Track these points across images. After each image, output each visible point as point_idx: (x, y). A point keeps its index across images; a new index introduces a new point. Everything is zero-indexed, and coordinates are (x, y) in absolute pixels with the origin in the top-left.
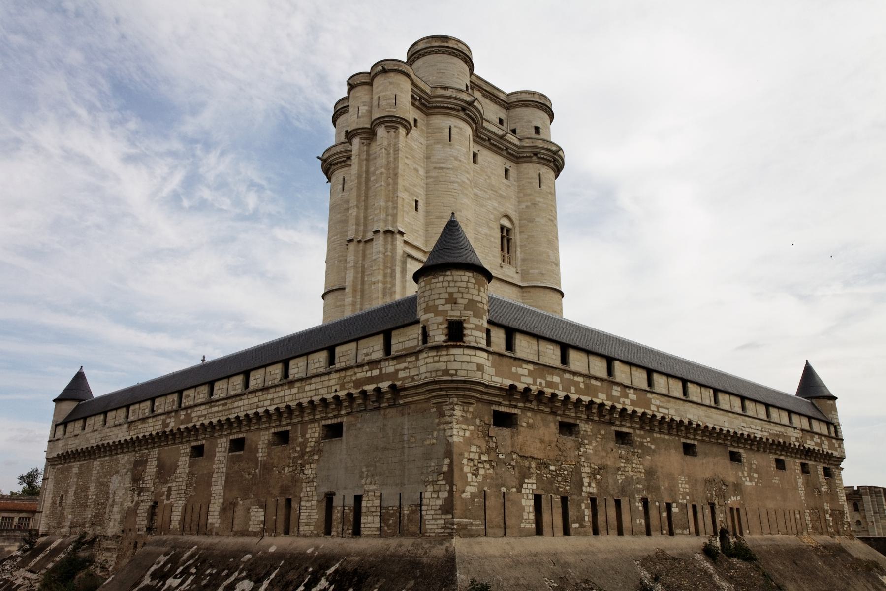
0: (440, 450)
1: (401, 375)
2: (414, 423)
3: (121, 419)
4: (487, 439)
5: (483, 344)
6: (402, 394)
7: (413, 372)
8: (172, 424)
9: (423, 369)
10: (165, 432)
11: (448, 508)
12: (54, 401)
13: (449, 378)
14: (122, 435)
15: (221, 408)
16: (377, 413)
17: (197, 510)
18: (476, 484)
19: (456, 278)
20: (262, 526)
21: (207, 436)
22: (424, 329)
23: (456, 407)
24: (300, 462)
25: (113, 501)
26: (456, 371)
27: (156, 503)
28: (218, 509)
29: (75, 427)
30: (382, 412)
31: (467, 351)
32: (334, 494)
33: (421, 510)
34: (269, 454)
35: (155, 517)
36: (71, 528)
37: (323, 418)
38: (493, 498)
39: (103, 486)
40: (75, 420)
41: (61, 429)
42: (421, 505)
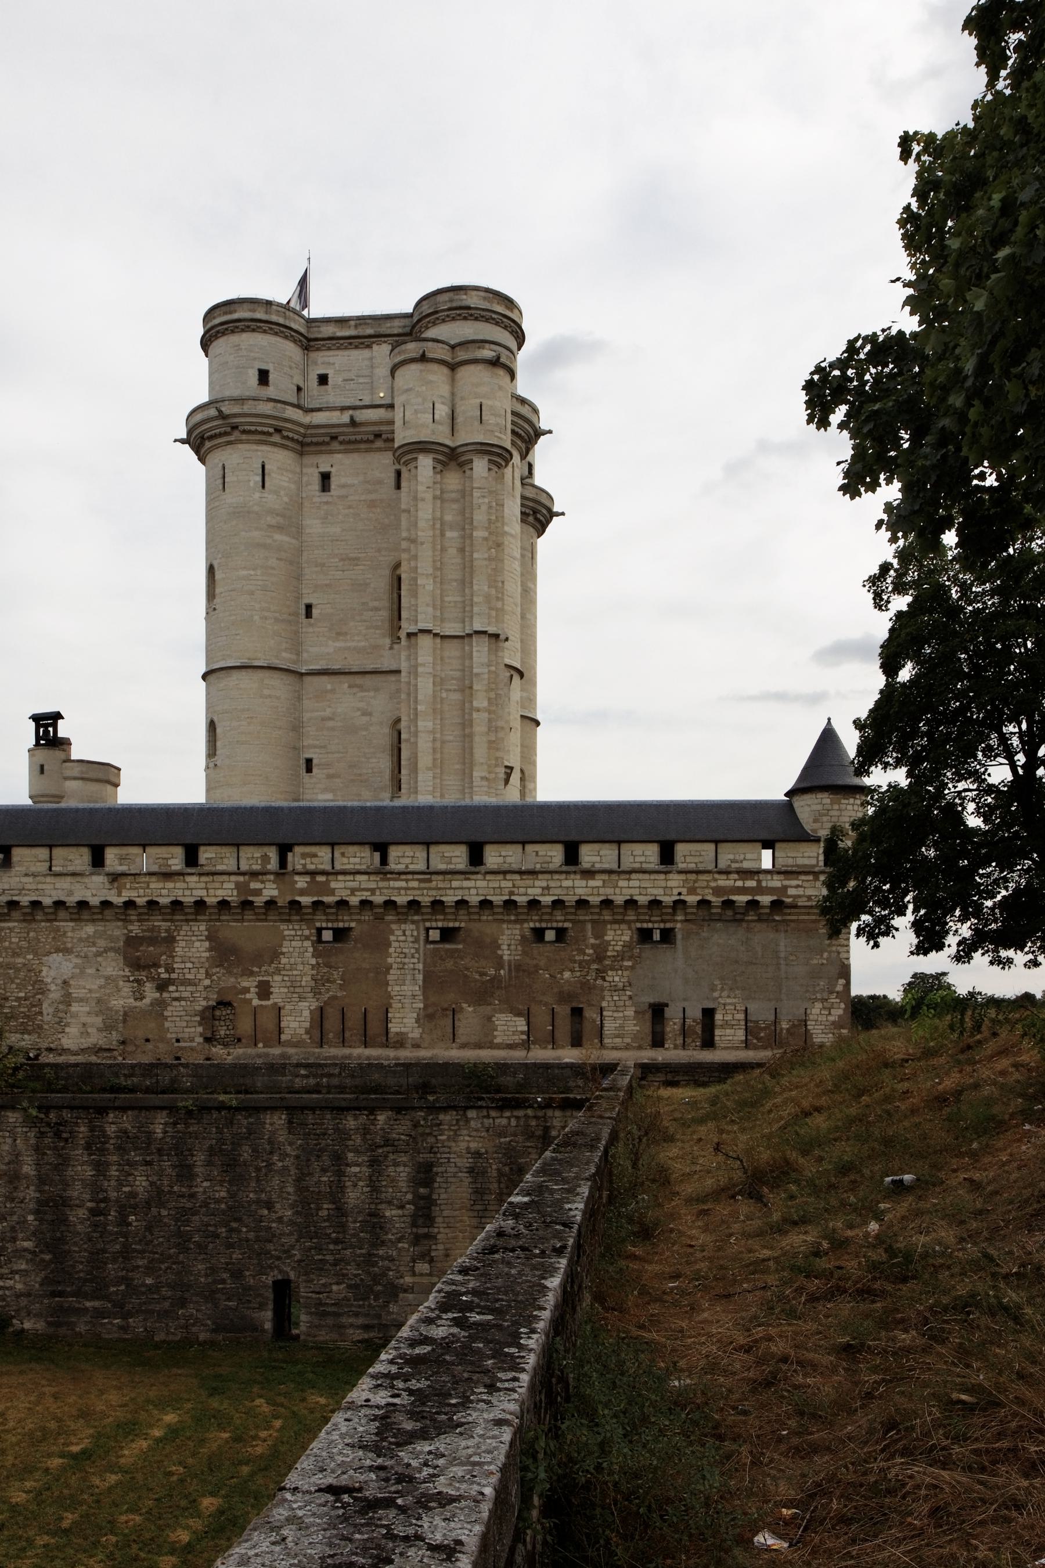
15: (415, 884)
24: (595, 966)
37: (638, 921)
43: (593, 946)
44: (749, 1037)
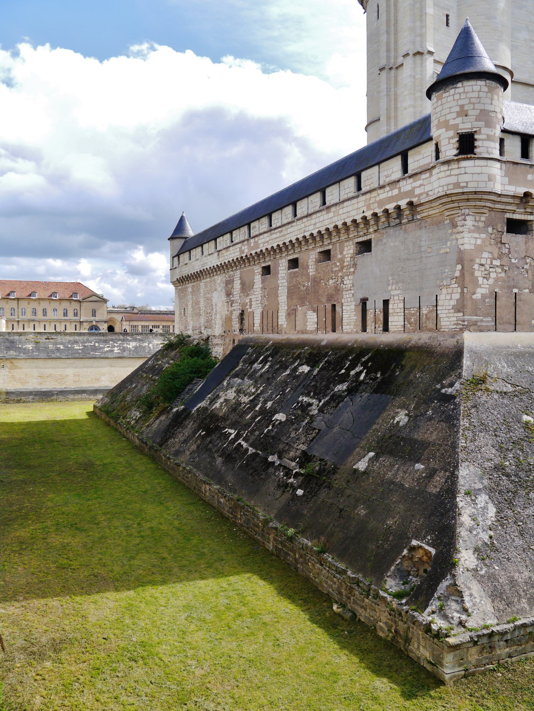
0: (454, 257)
1: (417, 192)
2: (430, 234)
3: (212, 250)
4: (499, 245)
5: (496, 154)
6: (419, 209)
7: (427, 188)
8: (246, 251)
9: (436, 184)
10: (242, 257)
11: (460, 308)
12: (169, 239)
13: (460, 190)
14: (214, 261)
16: (398, 228)
17: (270, 315)
18: (488, 286)
19: (467, 89)
20: (316, 326)
21: (272, 258)
22: (437, 145)
23: (467, 217)
24: (340, 274)
25: (216, 311)
26: (467, 183)
27: (243, 311)
28: (285, 314)
29: (185, 257)
30: (403, 227)
31: (478, 162)
32: (367, 300)
33: (437, 310)
34: (317, 270)
35: (244, 321)
36: (193, 330)
38: (504, 299)
39: (209, 300)
40: (184, 253)
41: (176, 259)
42: (437, 305)
43: (339, 260)
44: (406, 323)
